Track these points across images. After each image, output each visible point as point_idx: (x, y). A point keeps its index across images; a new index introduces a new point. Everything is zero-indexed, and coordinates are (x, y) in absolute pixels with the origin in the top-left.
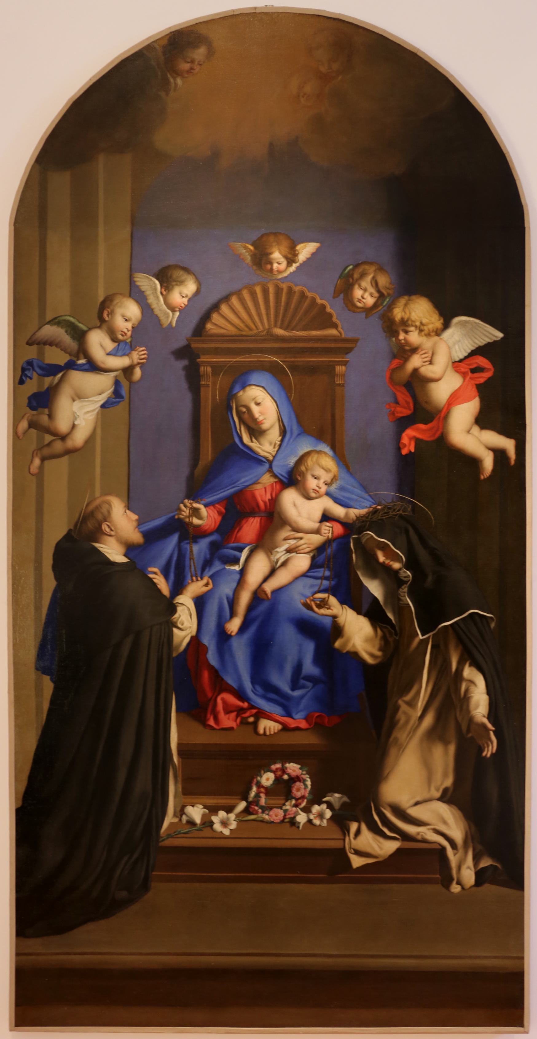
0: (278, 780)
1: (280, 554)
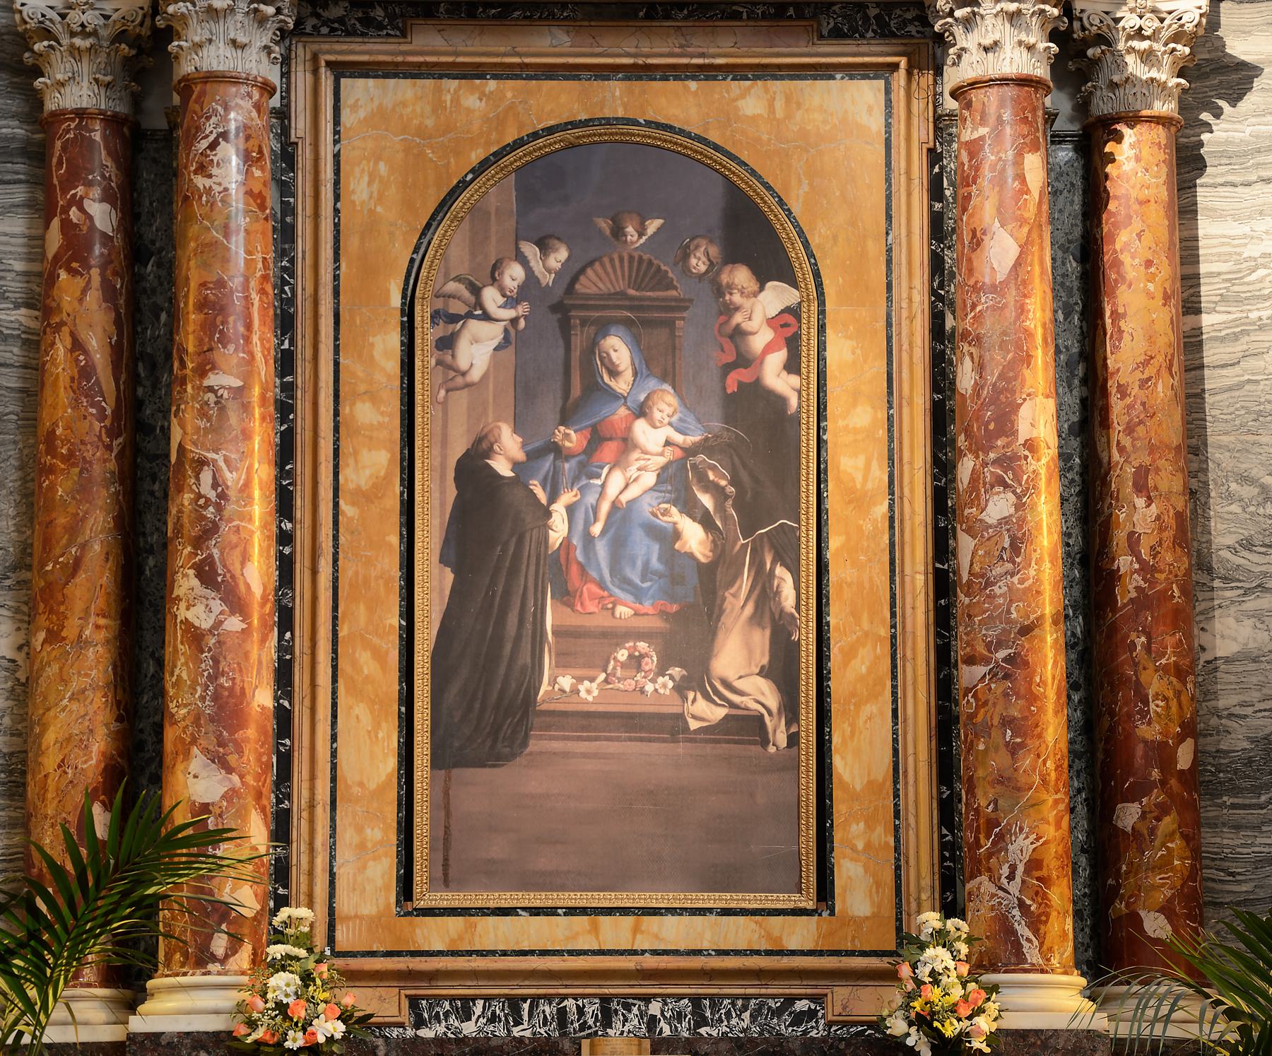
0: (631, 656)
1: (632, 471)
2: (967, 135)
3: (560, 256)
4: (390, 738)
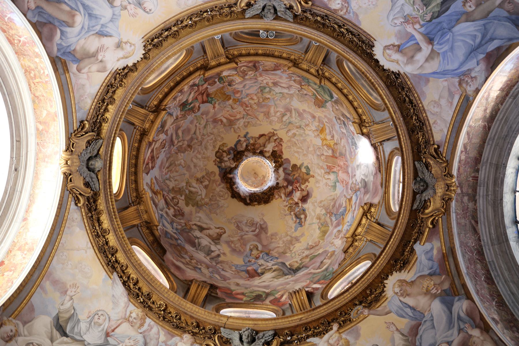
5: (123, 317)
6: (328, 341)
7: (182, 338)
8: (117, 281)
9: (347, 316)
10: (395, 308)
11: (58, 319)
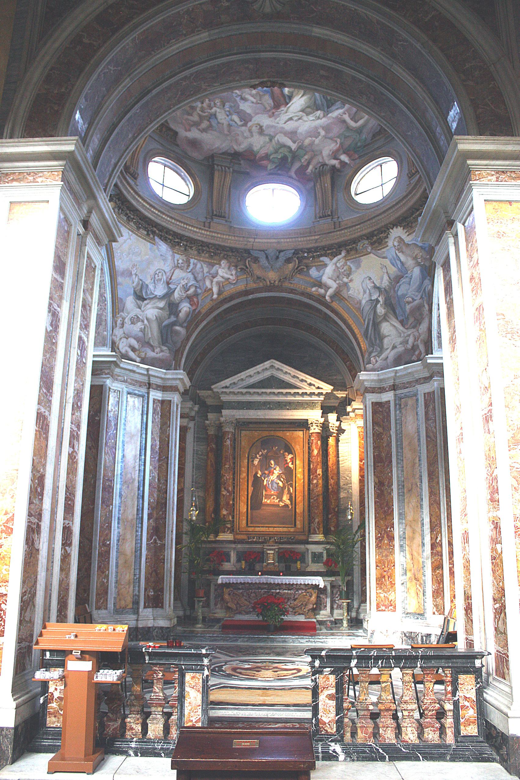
2: (312, 438)
3: (266, 451)
4: (246, 507)
5: (173, 266)
6: (336, 264)
7: (220, 265)
8: (160, 243)
9: (354, 245)
10: (391, 257)
11: (136, 293)
